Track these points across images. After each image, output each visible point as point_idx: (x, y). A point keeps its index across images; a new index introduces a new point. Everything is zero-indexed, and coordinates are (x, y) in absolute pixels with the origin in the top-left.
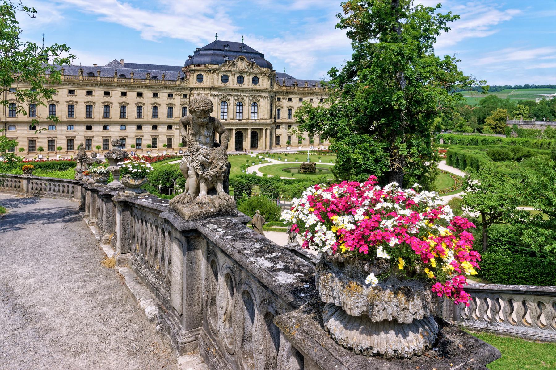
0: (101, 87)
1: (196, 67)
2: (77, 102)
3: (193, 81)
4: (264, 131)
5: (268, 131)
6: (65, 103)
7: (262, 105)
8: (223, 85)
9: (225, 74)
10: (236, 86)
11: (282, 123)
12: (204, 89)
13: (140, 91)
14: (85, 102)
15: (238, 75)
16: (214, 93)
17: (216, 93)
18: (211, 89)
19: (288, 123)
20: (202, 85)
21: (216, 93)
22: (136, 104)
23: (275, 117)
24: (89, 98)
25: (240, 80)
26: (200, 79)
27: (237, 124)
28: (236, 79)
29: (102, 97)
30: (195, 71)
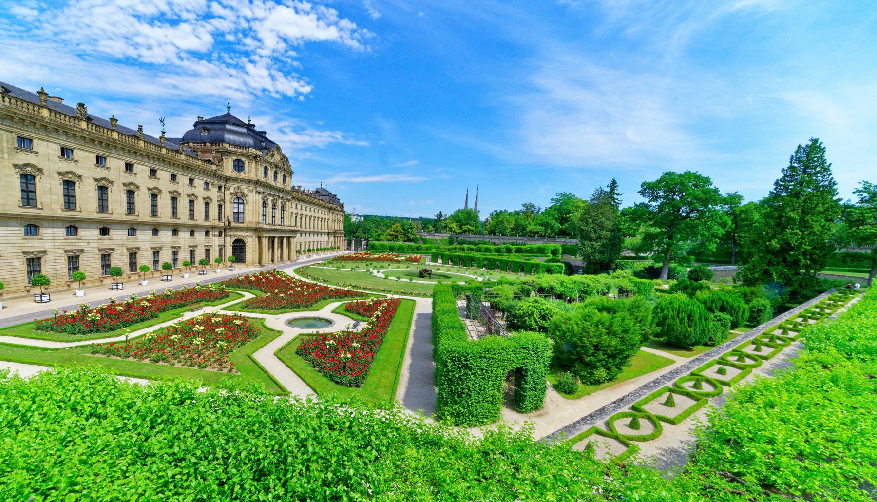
0: (121, 153)
1: (232, 149)
2: (80, 177)
3: (228, 168)
6: (56, 175)
12: (248, 181)
13: (174, 172)
14: (95, 180)
16: (260, 189)
18: (257, 183)
20: (243, 175)
22: (170, 193)
24: (100, 173)
26: (239, 166)
29: (122, 173)
30: (231, 153)
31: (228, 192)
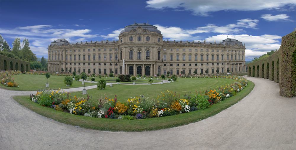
4: (152, 66)
5: (154, 66)
7: (152, 51)
8: (130, 42)
9: (131, 36)
10: (137, 42)
11: (167, 63)
15: (138, 36)
17: (126, 46)
18: (124, 44)
19: (170, 63)
21: (126, 46)
23: (162, 60)
24: (84, 53)
25: (139, 39)
27: (136, 62)
28: (137, 38)
31: (119, 50)
